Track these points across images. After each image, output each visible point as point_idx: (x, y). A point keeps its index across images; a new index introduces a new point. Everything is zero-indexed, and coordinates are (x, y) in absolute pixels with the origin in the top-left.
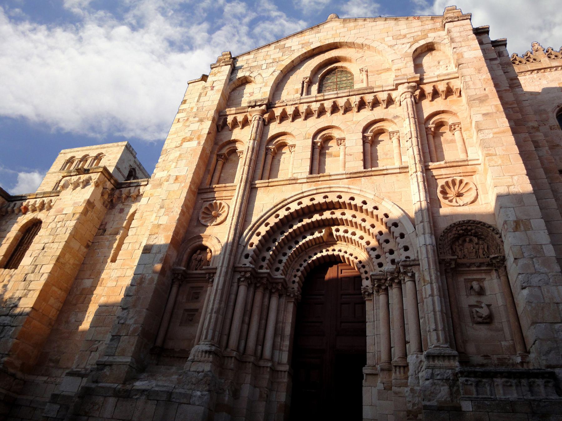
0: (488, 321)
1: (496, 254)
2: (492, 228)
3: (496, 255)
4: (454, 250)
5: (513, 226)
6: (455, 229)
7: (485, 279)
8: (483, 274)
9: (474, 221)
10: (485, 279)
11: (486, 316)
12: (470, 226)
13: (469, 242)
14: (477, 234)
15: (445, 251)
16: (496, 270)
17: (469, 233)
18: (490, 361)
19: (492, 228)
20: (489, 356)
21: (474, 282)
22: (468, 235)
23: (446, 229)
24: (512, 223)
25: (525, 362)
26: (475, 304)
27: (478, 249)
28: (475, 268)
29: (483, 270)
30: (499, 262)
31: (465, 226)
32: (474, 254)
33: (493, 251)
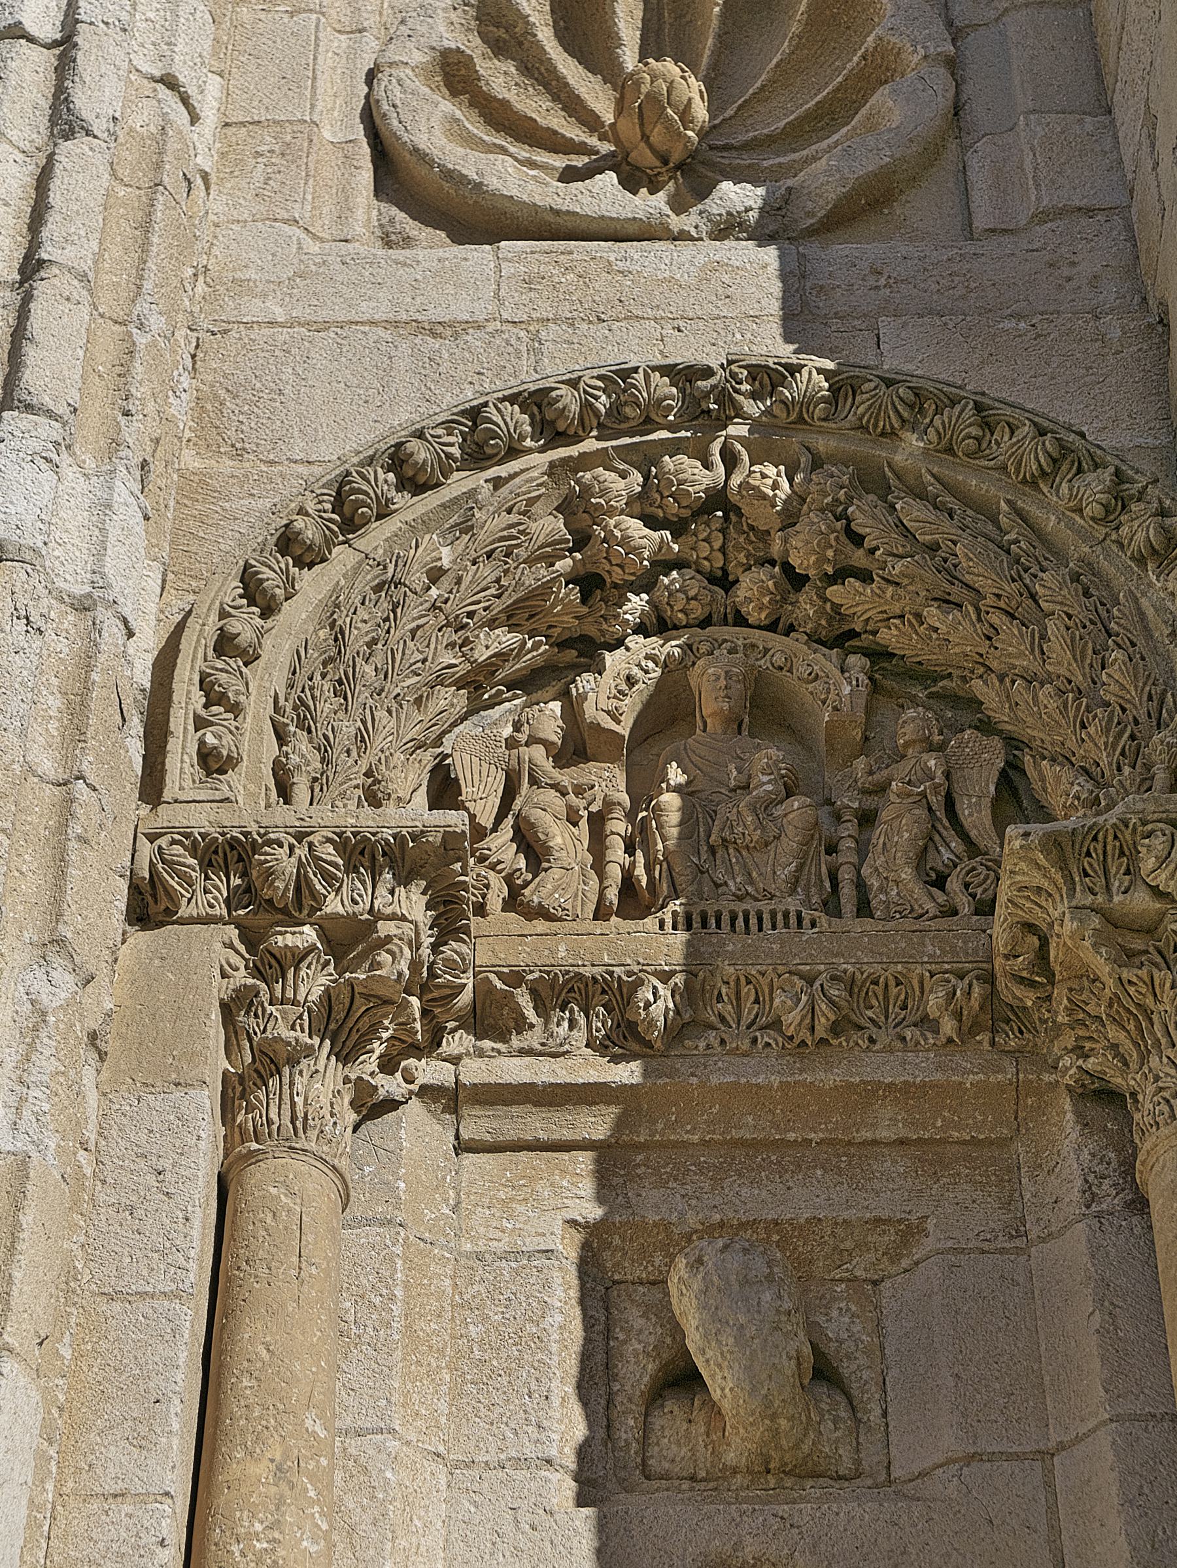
22: (740, 620)
29: (906, 1092)
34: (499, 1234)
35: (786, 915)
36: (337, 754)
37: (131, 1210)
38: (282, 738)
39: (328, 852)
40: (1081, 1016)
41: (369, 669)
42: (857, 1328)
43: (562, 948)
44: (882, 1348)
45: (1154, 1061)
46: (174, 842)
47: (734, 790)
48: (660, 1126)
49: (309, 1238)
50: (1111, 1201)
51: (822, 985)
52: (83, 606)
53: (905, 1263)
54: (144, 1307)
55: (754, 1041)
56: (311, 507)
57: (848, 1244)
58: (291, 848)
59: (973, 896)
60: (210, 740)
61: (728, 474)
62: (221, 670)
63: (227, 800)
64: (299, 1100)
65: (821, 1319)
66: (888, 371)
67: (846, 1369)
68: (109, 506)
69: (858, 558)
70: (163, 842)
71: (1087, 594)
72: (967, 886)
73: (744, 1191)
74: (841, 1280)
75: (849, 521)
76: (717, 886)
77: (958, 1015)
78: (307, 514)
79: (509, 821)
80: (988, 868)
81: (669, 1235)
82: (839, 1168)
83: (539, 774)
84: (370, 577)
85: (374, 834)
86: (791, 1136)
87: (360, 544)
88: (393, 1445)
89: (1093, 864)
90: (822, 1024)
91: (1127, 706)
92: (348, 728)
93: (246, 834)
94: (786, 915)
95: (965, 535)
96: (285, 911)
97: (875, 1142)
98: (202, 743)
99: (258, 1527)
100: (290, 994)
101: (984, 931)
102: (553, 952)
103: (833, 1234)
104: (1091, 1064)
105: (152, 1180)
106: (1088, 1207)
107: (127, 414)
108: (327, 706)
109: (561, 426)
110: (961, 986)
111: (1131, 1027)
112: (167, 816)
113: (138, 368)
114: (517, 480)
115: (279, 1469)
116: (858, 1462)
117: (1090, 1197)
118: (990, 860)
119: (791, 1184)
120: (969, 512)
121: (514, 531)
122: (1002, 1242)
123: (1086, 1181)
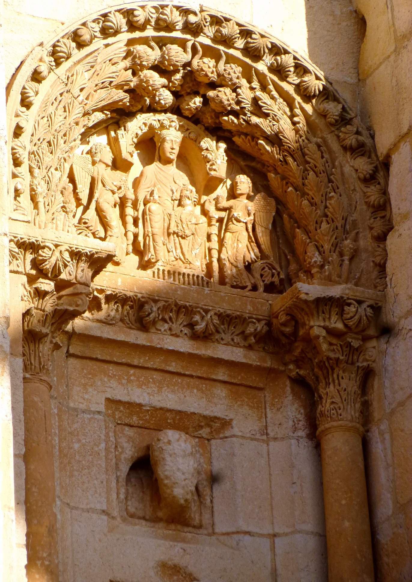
3: (336, 291)
7: (226, 424)
8: (221, 392)
10: (226, 424)
12: (208, 51)
15: (41, 189)
21: (171, 434)
31: (182, 44)
33: (317, 258)
34: (82, 401)
40: (304, 355)
48: (142, 361)
51: (211, 317)
53: (221, 435)
55: (181, 331)
57: (203, 424)
59: (263, 281)
61: (193, 57)
62: (19, 147)
72: (262, 276)
73: (170, 396)
74: (198, 437)
78: (44, 62)
80: (269, 269)
81: (141, 409)
82: (202, 390)
85: (83, 250)
86: (187, 373)
89: (328, 307)
91: (335, 220)
93: (37, 241)
95: (279, 113)
101: (268, 301)
103: (199, 420)
104: (302, 372)
106: (294, 433)
111: (325, 372)
116: (201, 521)
117: (295, 430)
118: (269, 264)
119: (185, 394)
121: (114, 75)
122: (258, 436)
123: (294, 421)
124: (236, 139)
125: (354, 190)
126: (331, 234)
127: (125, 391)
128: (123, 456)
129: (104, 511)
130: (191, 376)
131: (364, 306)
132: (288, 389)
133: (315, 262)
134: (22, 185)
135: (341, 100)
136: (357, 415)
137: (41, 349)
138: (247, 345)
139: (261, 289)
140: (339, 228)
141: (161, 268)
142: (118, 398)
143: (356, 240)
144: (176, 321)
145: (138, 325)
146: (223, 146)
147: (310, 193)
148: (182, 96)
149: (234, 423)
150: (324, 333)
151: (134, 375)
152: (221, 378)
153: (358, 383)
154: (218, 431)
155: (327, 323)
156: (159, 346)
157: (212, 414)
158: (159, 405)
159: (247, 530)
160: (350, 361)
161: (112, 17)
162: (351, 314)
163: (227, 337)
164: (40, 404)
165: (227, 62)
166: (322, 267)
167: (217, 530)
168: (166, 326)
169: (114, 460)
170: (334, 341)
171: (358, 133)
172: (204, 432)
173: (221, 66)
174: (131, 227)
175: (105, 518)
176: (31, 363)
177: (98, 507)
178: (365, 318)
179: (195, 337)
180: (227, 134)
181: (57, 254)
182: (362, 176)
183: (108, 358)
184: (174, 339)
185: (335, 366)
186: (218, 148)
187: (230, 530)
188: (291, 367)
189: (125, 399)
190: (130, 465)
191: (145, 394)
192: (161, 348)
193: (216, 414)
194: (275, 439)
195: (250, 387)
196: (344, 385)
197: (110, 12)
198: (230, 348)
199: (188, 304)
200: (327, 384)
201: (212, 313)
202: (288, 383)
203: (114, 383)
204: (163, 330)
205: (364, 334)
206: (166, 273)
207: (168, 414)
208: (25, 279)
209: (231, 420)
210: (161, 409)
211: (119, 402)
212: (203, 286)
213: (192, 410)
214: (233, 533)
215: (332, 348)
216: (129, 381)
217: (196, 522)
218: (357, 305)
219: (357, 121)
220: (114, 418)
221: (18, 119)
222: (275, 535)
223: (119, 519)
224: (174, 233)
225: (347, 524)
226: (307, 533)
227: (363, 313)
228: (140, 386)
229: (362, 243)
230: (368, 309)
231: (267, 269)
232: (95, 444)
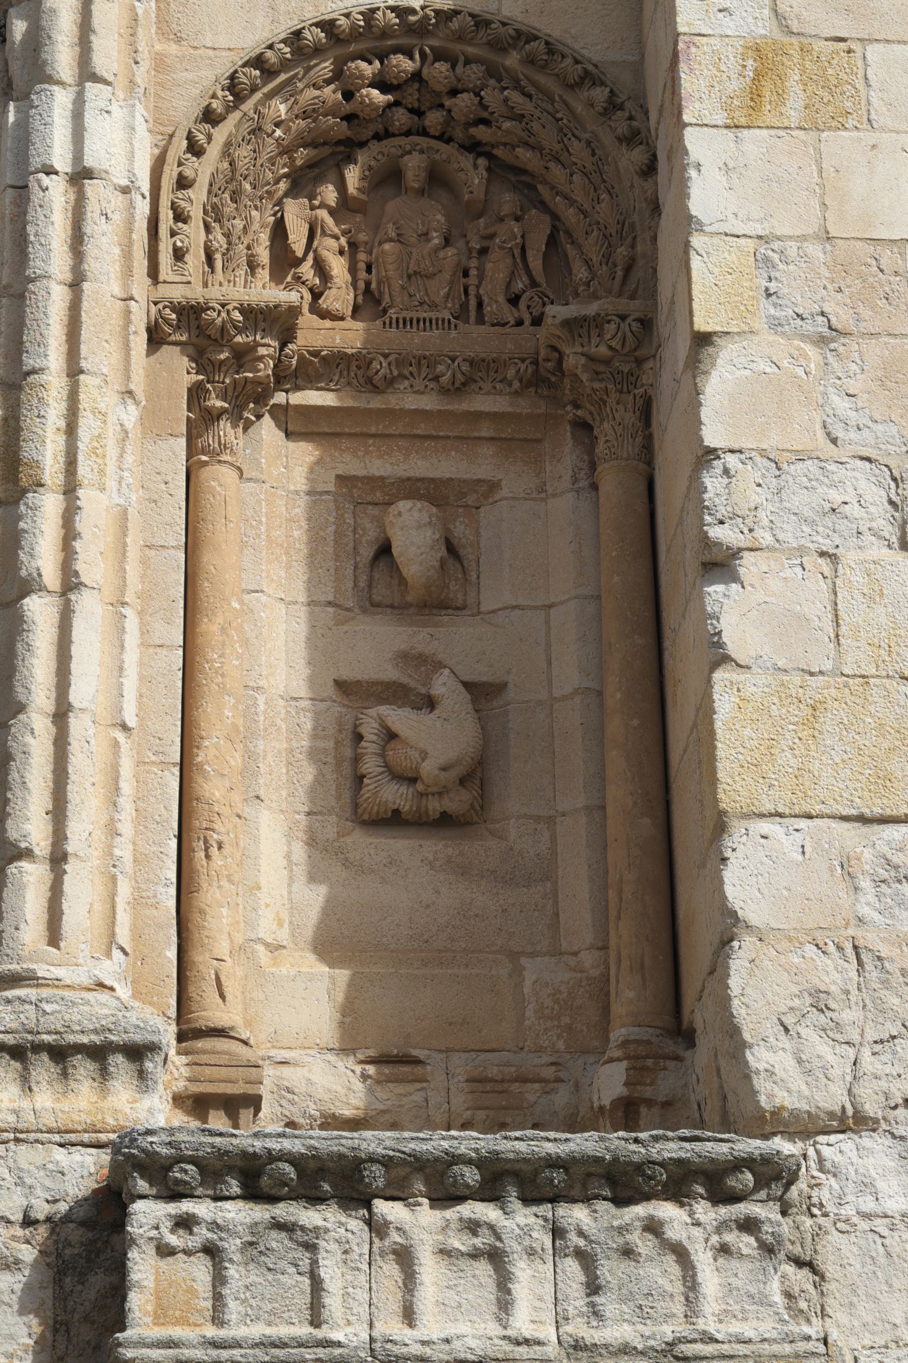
0: (456, 802)
1: (596, 297)
2: (600, 94)
3: (592, 309)
4: (297, 239)
5: (734, 85)
6: (325, 68)
7: (493, 486)
8: (487, 450)
9: (480, 22)
10: (493, 486)
11: (444, 769)
12: (440, 55)
13: (421, 192)
14: (481, 133)
16: (583, 427)
17: (433, 119)
18: (418, 1097)
19: (600, 94)
20: (417, 1062)
21: (403, 505)
22: (424, 133)
23: (258, 62)
24: (731, 63)
25: (650, 1103)
26: (392, 674)
27: (483, 251)
28: (428, 402)
29: (494, 417)
30: (607, 362)
32: (439, 289)
35: (443, 320)
36: (234, 239)
37: (155, 501)
38: (208, 228)
39: (237, 316)
41: (248, 187)
42: (467, 532)
43: (338, 338)
44: (478, 543)
45: (606, 424)
46: (165, 307)
47: (420, 236)
49: (229, 508)
50: (584, 483)
52: (125, 191)
54: (165, 553)
56: (220, 93)
57: (465, 490)
58: (219, 312)
59: (531, 313)
60: (179, 244)
63: (189, 283)
64: (222, 433)
65: (451, 526)
66: (505, 17)
67: (462, 552)
68: (133, 129)
69: (485, 115)
70: (160, 306)
71: (594, 154)
72: (529, 307)
75: (482, 98)
76: (410, 296)
77: (521, 381)
78: (217, 98)
79: (311, 256)
83: (326, 229)
84: (246, 126)
86: (441, 434)
87: (243, 107)
88: (263, 598)
89: (585, 328)
90: (457, 384)
92: (239, 223)
94: (443, 320)
96: (216, 340)
97: (480, 438)
98: (174, 244)
99: (215, 656)
100: (217, 378)
102: (334, 339)
104: (579, 413)
105: (163, 486)
107: (136, 63)
108: (229, 208)
109: (342, 37)
110: (523, 367)
112: (164, 291)
113: (140, 31)
114: (318, 68)
115: (223, 628)
116: (465, 601)
117: (575, 480)
120: (540, 96)
122: (534, 495)
124: (495, 152)
125: (632, 186)
126: (600, 243)
127: (362, 464)
128: (364, 540)
129: (329, 603)
130: (448, 437)
131: (628, 320)
132: (569, 434)
133: (581, 279)
134: (182, 242)
135: (608, 83)
136: (636, 451)
137: (222, 426)
138: (512, 390)
139: (527, 323)
140: (614, 234)
141: (394, 316)
142: (353, 473)
143: (633, 246)
144: (419, 375)
145: (370, 387)
146: (482, 162)
147: (579, 199)
148: (424, 113)
149: (504, 482)
150: (583, 360)
151: (373, 445)
152: (484, 434)
153: (638, 413)
154: (486, 497)
155: (586, 349)
156: (397, 407)
157: (475, 477)
158: (406, 474)
159: (515, 604)
160: (625, 389)
161: (307, 34)
162: (613, 332)
163: (486, 386)
164: (218, 489)
165: (467, 62)
166: (588, 284)
167: (482, 609)
168: (406, 383)
169: (351, 545)
170: (602, 368)
171: (631, 118)
172: (470, 500)
173: (459, 69)
174: (363, 275)
175: (331, 610)
176: (209, 445)
177: (323, 598)
178: (629, 334)
179: (445, 392)
180: (487, 149)
181: (224, 315)
182: (637, 169)
183: (338, 430)
184: (418, 397)
185: (605, 397)
186: (476, 166)
187: (496, 607)
188: (569, 408)
189: (361, 473)
190: (375, 547)
191: (388, 465)
192: (401, 409)
193: (480, 477)
194: (554, 495)
195: (526, 440)
196: (618, 420)
197: (304, 28)
198: (492, 397)
199: (427, 353)
200: (602, 420)
201: (459, 360)
202: (568, 428)
203: (347, 457)
204: (402, 387)
205: (636, 354)
206: (401, 321)
207: (419, 484)
208: (191, 350)
209: (500, 480)
210: (409, 479)
211: (355, 478)
212: (449, 329)
213: (448, 475)
214: (500, 609)
215: (600, 377)
216: (367, 452)
217: (460, 603)
218: (617, 320)
219: (628, 105)
220: (352, 497)
221: (181, 168)
222: (551, 606)
223: (357, 610)
224: (415, 273)
225: (616, 579)
226: (585, 597)
227: (627, 329)
228: (380, 457)
229: (639, 248)
230: (634, 324)
231: (536, 298)
232: (321, 529)
